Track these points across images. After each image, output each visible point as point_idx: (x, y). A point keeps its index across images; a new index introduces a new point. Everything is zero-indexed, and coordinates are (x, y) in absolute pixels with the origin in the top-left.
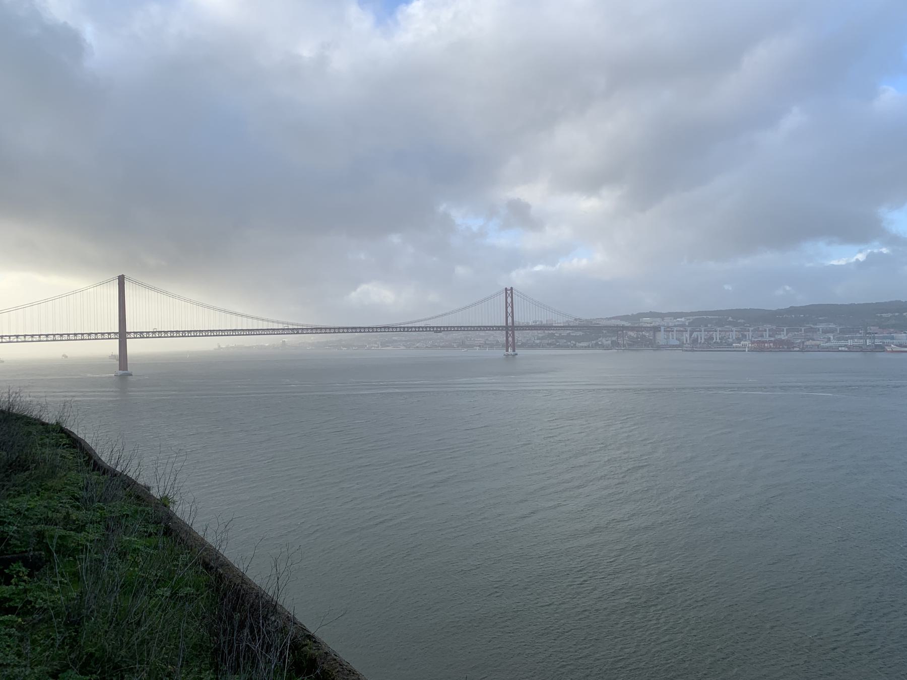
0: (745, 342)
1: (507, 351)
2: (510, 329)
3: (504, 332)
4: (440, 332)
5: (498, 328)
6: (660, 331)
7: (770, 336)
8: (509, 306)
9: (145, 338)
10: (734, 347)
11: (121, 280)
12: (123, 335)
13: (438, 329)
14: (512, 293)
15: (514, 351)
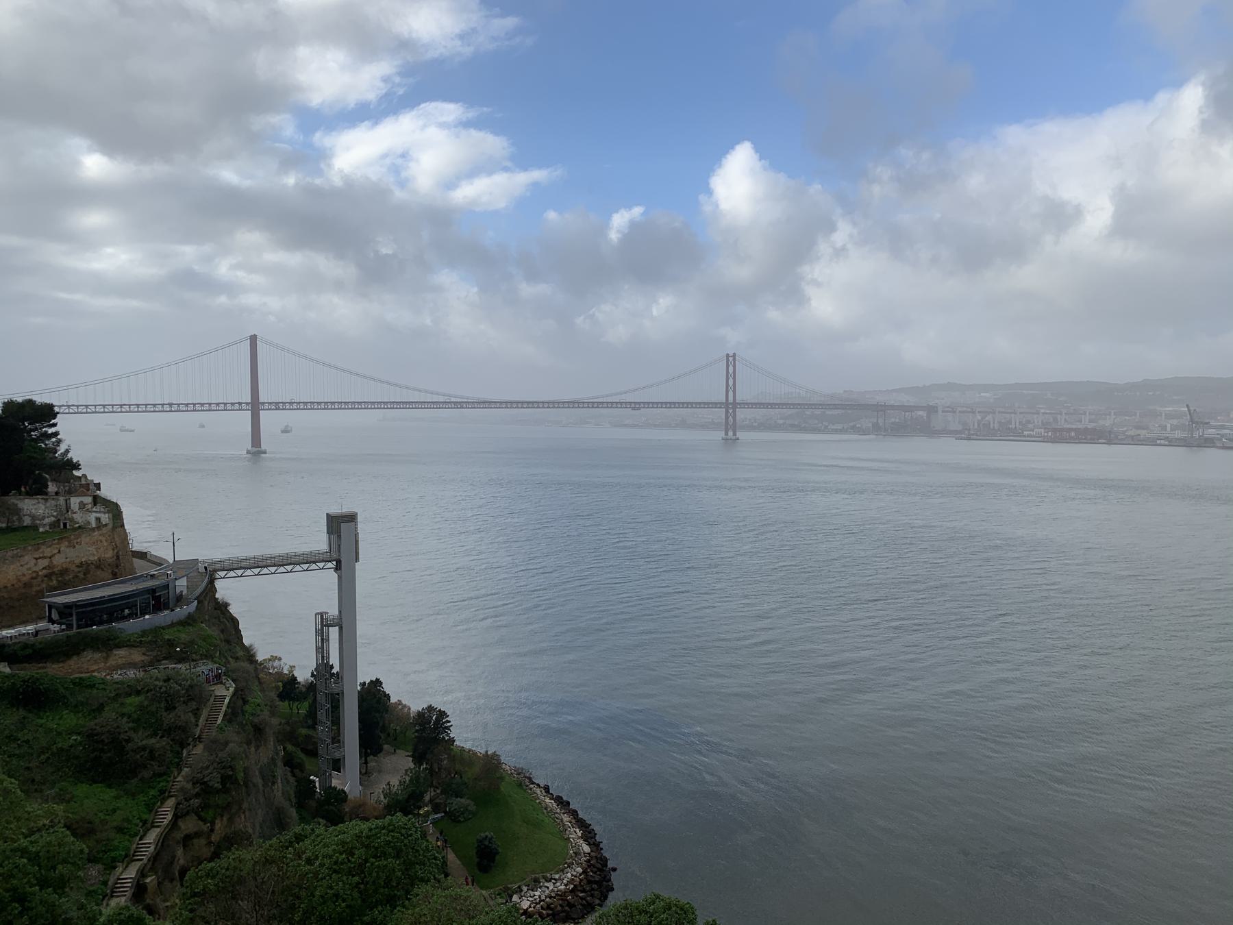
0: (1040, 430)
1: (726, 434)
2: (730, 406)
3: (724, 409)
4: (639, 409)
5: (715, 405)
6: (937, 412)
7: (1090, 421)
8: (731, 376)
9: (281, 409)
10: (1025, 436)
11: (253, 339)
12: (255, 406)
13: (636, 406)
14: (734, 360)
15: (735, 434)
